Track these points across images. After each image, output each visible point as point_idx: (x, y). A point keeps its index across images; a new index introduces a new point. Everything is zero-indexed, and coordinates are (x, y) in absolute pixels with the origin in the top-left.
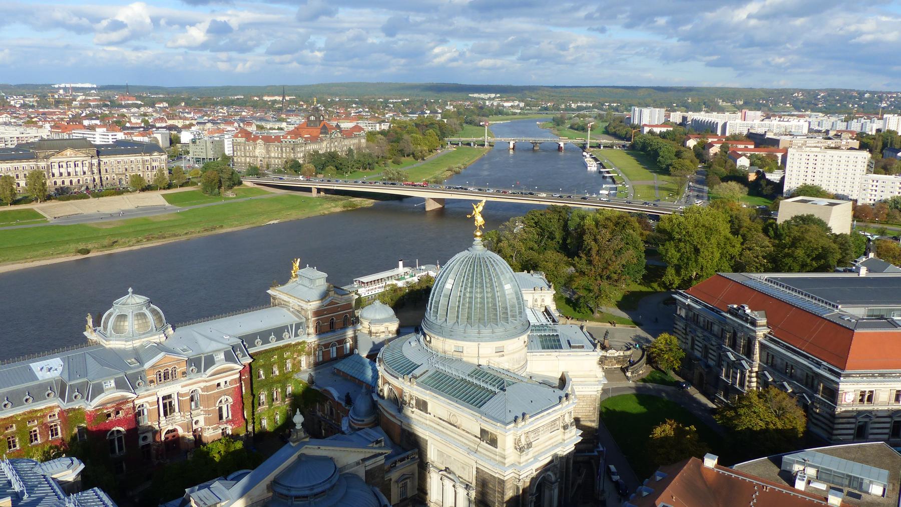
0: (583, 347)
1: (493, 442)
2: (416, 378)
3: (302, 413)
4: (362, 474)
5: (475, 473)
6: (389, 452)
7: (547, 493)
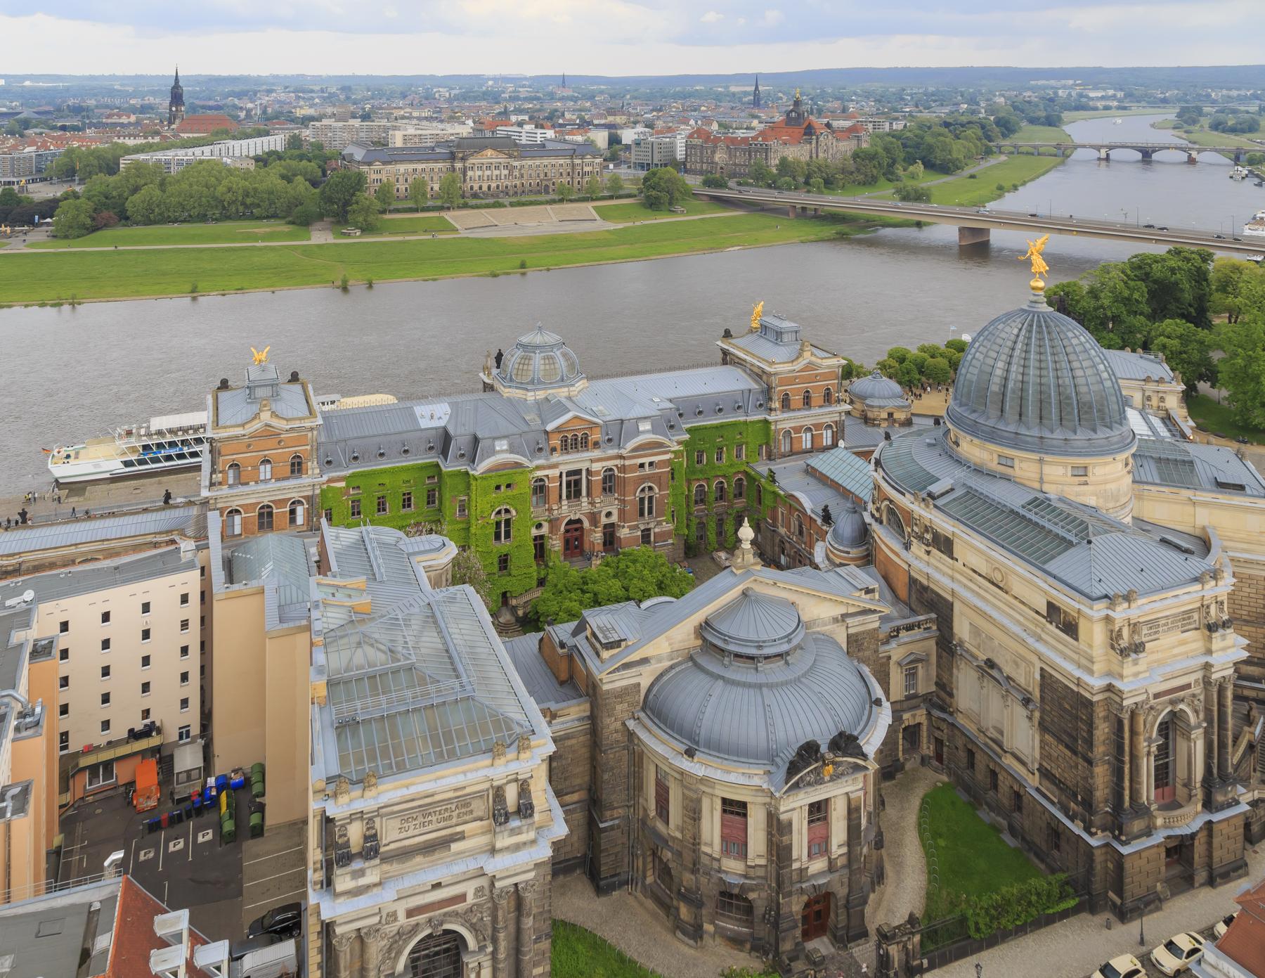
0: (1240, 488)
1: (1070, 628)
2: (934, 498)
3: (757, 527)
4: (842, 640)
5: (1038, 677)
6: (887, 610)
7: (1182, 745)
